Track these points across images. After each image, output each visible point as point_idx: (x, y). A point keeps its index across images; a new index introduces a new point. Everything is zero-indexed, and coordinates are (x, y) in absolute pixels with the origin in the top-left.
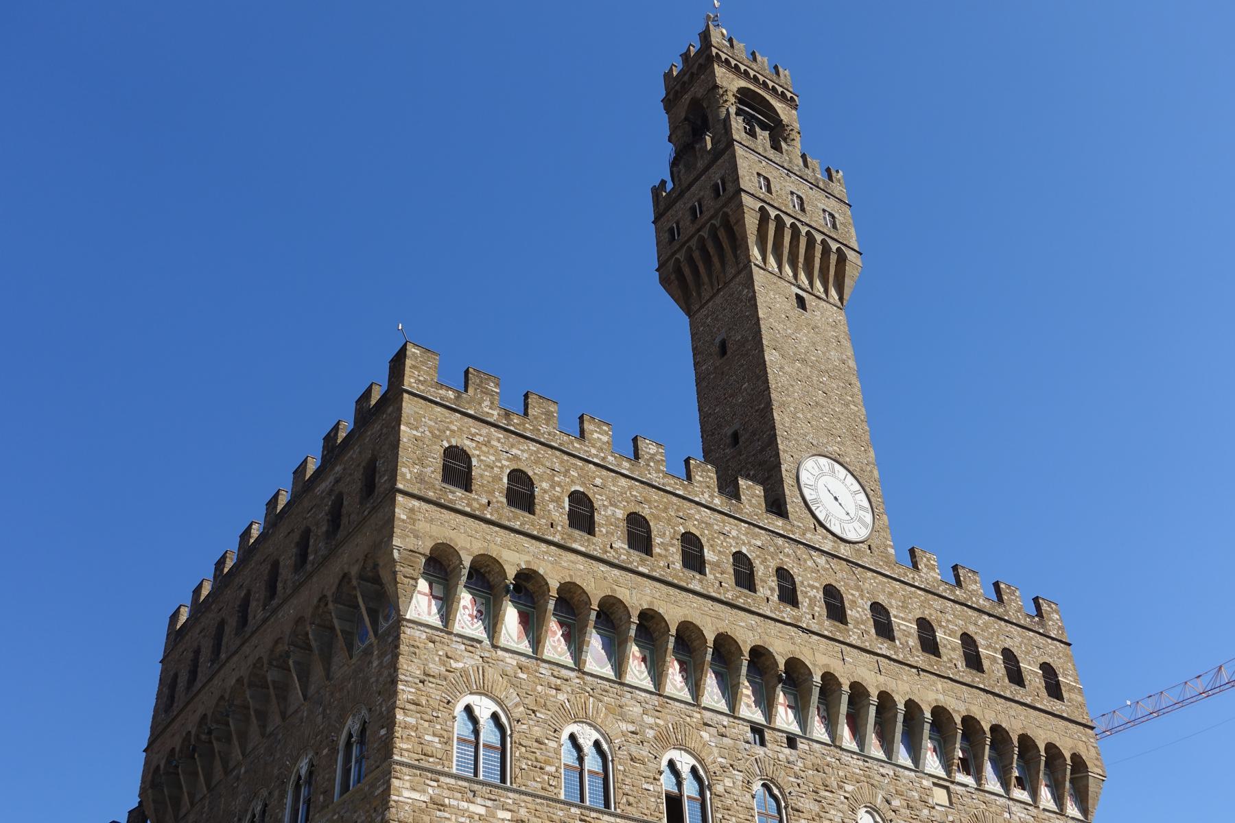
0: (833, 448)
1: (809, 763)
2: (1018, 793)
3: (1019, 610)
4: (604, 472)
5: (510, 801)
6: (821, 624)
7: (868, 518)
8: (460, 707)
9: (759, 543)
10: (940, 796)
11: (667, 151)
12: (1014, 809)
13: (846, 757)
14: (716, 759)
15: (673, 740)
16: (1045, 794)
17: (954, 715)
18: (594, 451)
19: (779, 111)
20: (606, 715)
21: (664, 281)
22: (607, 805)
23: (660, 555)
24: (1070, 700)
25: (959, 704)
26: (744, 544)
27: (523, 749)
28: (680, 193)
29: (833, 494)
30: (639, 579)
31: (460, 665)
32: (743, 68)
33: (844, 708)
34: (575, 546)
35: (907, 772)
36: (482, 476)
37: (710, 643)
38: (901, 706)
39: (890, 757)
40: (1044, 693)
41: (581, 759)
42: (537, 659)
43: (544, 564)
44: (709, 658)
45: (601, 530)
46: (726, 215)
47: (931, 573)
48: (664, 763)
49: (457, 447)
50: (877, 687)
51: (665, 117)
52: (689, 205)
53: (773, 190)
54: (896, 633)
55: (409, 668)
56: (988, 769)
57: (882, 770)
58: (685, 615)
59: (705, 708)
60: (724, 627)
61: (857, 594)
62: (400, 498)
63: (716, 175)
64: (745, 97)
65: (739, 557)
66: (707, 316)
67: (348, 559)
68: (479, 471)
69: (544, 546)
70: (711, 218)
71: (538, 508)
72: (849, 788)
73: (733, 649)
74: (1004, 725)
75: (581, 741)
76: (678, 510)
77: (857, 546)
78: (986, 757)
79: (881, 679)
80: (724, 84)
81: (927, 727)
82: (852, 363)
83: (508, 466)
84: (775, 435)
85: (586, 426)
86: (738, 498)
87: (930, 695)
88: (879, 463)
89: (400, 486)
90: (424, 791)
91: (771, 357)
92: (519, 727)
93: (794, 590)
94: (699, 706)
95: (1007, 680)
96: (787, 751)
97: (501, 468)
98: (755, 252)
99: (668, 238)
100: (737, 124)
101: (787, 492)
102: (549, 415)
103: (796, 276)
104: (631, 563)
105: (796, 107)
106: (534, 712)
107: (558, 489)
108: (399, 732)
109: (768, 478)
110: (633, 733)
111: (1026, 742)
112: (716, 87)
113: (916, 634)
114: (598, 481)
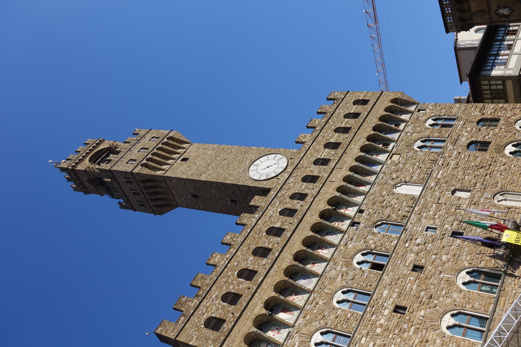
1: (371, 207)
2: (401, 127)
3: (330, 107)
4: (233, 260)
5: (358, 336)
6: (317, 187)
7: (279, 156)
9: (278, 203)
10: (396, 158)
11: (106, 198)
12: (407, 130)
13: (372, 191)
14: (360, 244)
15: (349, 260)
16: (403, 117)
17: (365, 144)
18: (223, 262)
19: (104, 147)
20: (333, 286)
21: (161, 213)
22: (369, 295)
23: (272, 246)
24: (370, 97)
25: (361, 140)
26: (277, 209)
27: (338, 325)
28: (125, 197)
29: (266, 168)
30: (280, 257)
31: (297, 343)
32: (81, 158)
33: (352, 187)
34: (260, 281)
35: (383, 168)
36: (220, 314)
37: (313, 234)
38: (357, 164)
39: (376, 174)
40: (365, 106)
41: (348, 301)
42: (303, 309)
43: (264, 296)
44: (319, 236)
45: (256, 268)
46: (140, 181)
47: (308, 138)
48: (357, 266)
49: (205, 322)
50: (347, 171)
51: (92, 195)
52: (132, 195)
53: (135, 159)
54: (328, 158)
56: (389, 136)
57: (380, 178)
58: (300, 241)
59: (339, 243)
60: (308, 227)
61: (308, 169)
63: (122, 180)
64: (93, 160)
65: (282, 213)
66: (180, 200)
68: (218, 314)
69: (257, 294)
70: (140, 187)
71: (240, 293)
72: (384, 193)
73: (318, 225)
74: (374, 125)
75: (341, 299)
76: (256, 233)
77: (289, 164)
78: (385, 136)
79: (344, 168)
80: (85, 167)
81: (367, 156)
82: (215, 146)
83: (219, 301)
84: (237, 186)
85: (212, 262)
86: (258, 207)
87: (355, 151)
88: (258, 146)
91: (203, 178)
92: (329, 324)
93: (301, 194)
94: (338, 246)
95: (356, 119)
96: (364, 214)
97: (219, 304)
98: (159, 173)
99: (143, 207)
100: (104, 166)
101: (260, 186)
102: (202, 278)
103: (173, 159)
104: (273, 258)
105: (104, 140)
106: (324, 316)
107: (234, 282)
109: (253, 192)
110: (342, 276)
111: (382, 118)
112: (85, 171)
113: (330, 150)
114: (236, 264)
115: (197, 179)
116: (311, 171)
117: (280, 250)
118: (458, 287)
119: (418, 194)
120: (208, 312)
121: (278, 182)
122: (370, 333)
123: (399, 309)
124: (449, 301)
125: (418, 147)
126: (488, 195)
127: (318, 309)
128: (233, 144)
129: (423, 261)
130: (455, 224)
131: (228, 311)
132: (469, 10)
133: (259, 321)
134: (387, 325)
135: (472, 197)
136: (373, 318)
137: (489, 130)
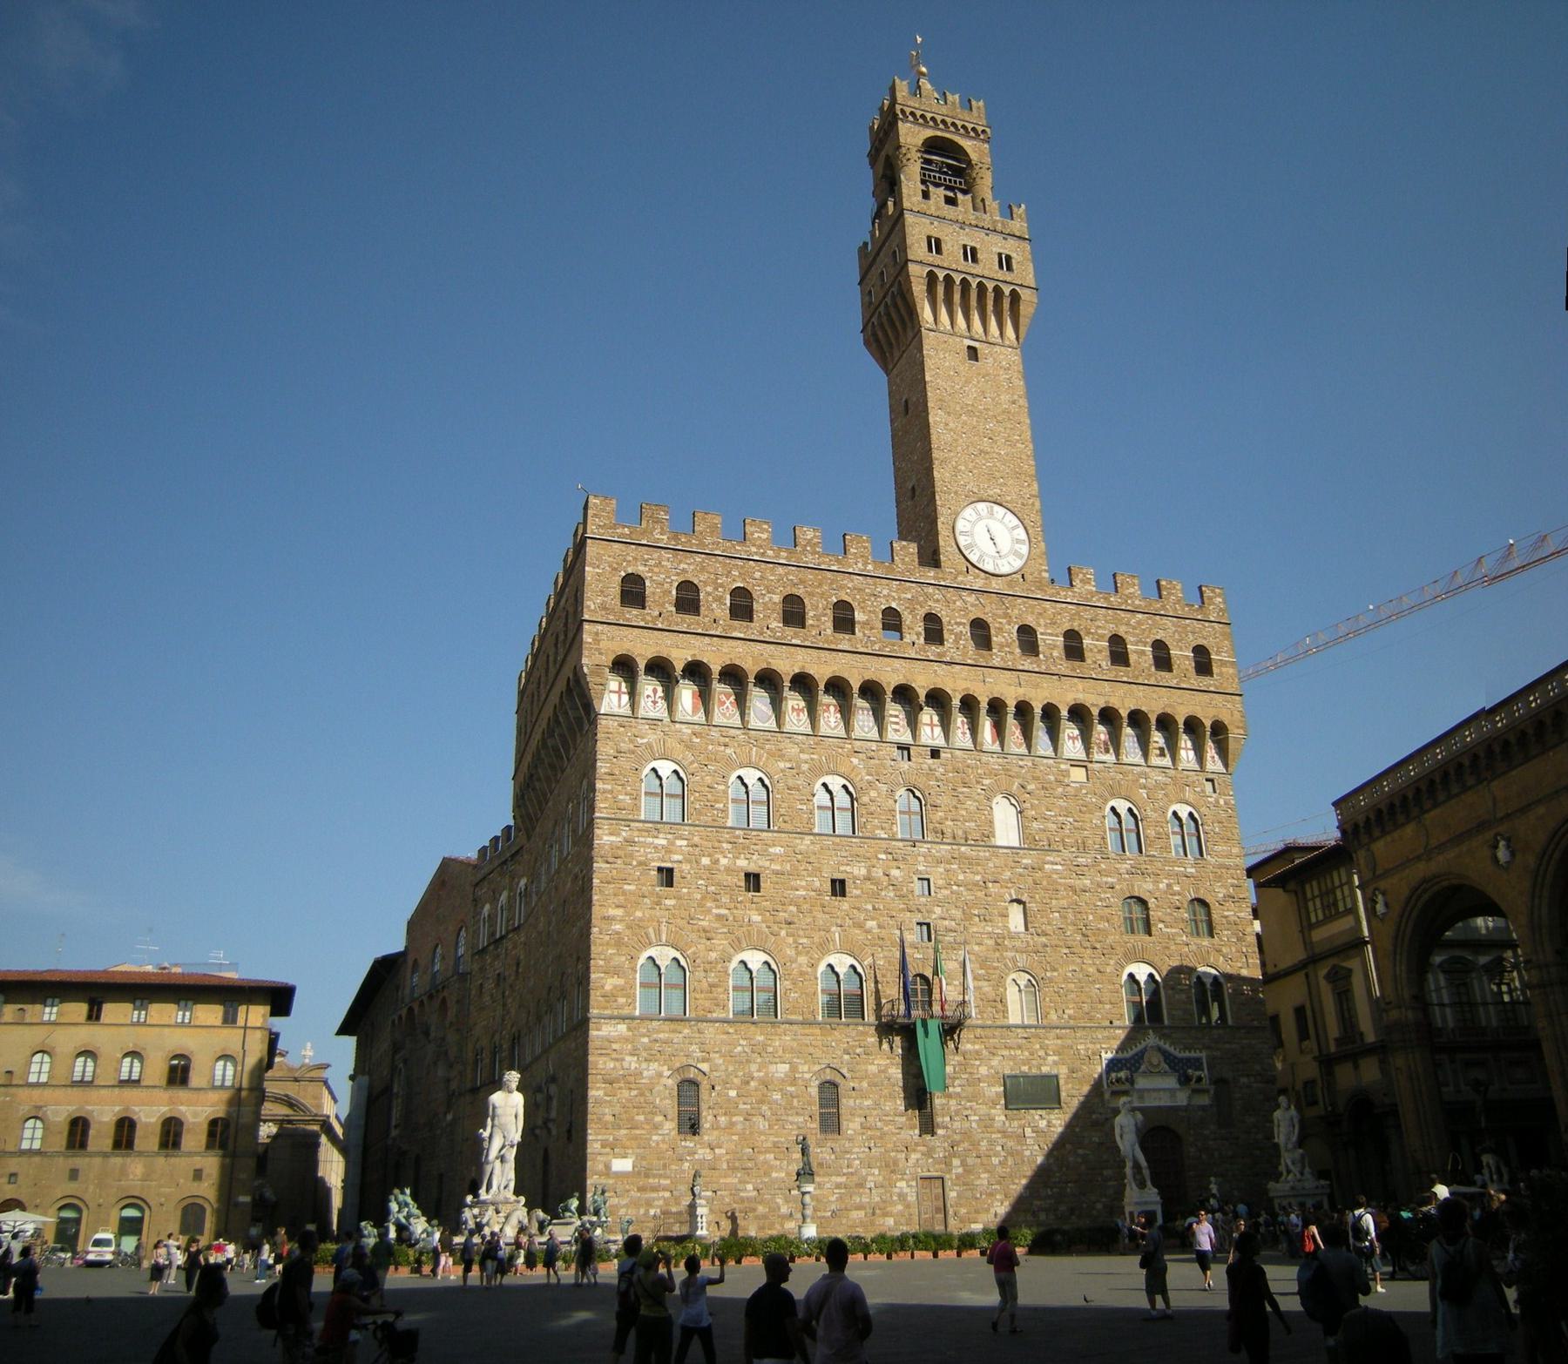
0: (994, 492)
2: (1155, 760)
3: (1178, 602)
7: (1024, 549)
8: (647, 770)
10: (1078, 775)
13: (985, 758)
16: (1187, 754)
18: (754, 549)
19: (969, 151)
21: (867, 343)
24: (1221, 674)
25: (1095, 701)
29: (990, 537)
30: (792, 649)
47: (1087, 584)
55: (604, 749)
62: (586, 626)
67: (567, 672)
72: (986, 782)
79: (1021, 691)
82: (1023, 402)
84: (934, 494)
85: (748, 529)
87: (1064, 695)
89: (586, 617)
90: (618, 835)
91: (936, 417)
94: (849, 738)
101: (941, 543)
105: (987, 141)
108: (599, 796)
114: (758, 575)
115: (930, 405)
116: (1000, 629)
118: (819, 960)
119: (999, 843)
120: (650, 571)
121: (960, 573)
123: (753, 881)
124: (790, 952)
125: (1113, 809)
126: (1022, 960)
128: (1034, 439)
129: (858, 892)
130: (946, 923)
131: (663, 605)
132: (1373, 840)
135: (1013, 936)
137: (1182, 925)
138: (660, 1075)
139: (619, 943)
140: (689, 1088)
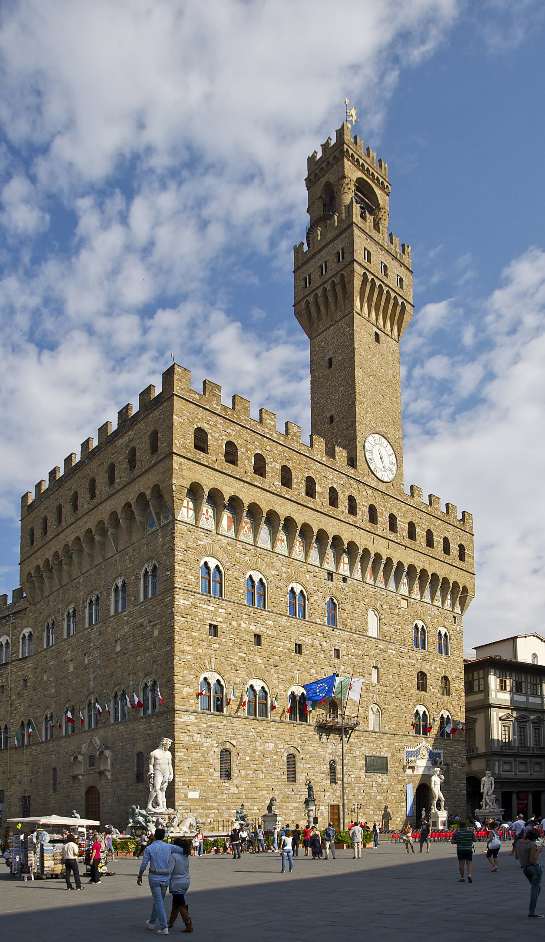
4: (271, 442)
5: (224, 605)
14: (311, 587)
18: (267, 431)
20: (266, 567)
34: (257, 484)
45: (269, 475)
75: (254, 579)
96: (342, 584)
107: (249, 452)
114: (268, 448)
117: (292, 499)
122: (230, 616)
127: (240, 557)
133: (215, 493)
134: (241, 630)
136: (244, 615)
138: (212, 746)
139: (190, 668)
140: (226, 754)
